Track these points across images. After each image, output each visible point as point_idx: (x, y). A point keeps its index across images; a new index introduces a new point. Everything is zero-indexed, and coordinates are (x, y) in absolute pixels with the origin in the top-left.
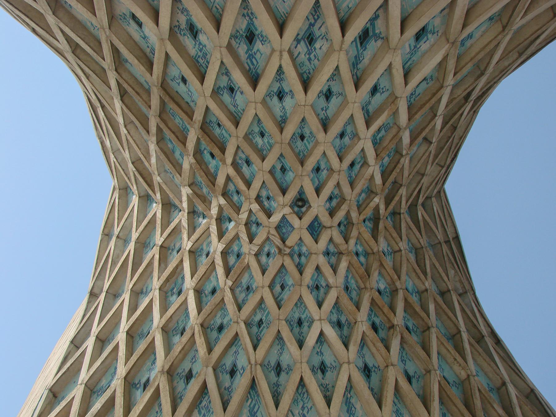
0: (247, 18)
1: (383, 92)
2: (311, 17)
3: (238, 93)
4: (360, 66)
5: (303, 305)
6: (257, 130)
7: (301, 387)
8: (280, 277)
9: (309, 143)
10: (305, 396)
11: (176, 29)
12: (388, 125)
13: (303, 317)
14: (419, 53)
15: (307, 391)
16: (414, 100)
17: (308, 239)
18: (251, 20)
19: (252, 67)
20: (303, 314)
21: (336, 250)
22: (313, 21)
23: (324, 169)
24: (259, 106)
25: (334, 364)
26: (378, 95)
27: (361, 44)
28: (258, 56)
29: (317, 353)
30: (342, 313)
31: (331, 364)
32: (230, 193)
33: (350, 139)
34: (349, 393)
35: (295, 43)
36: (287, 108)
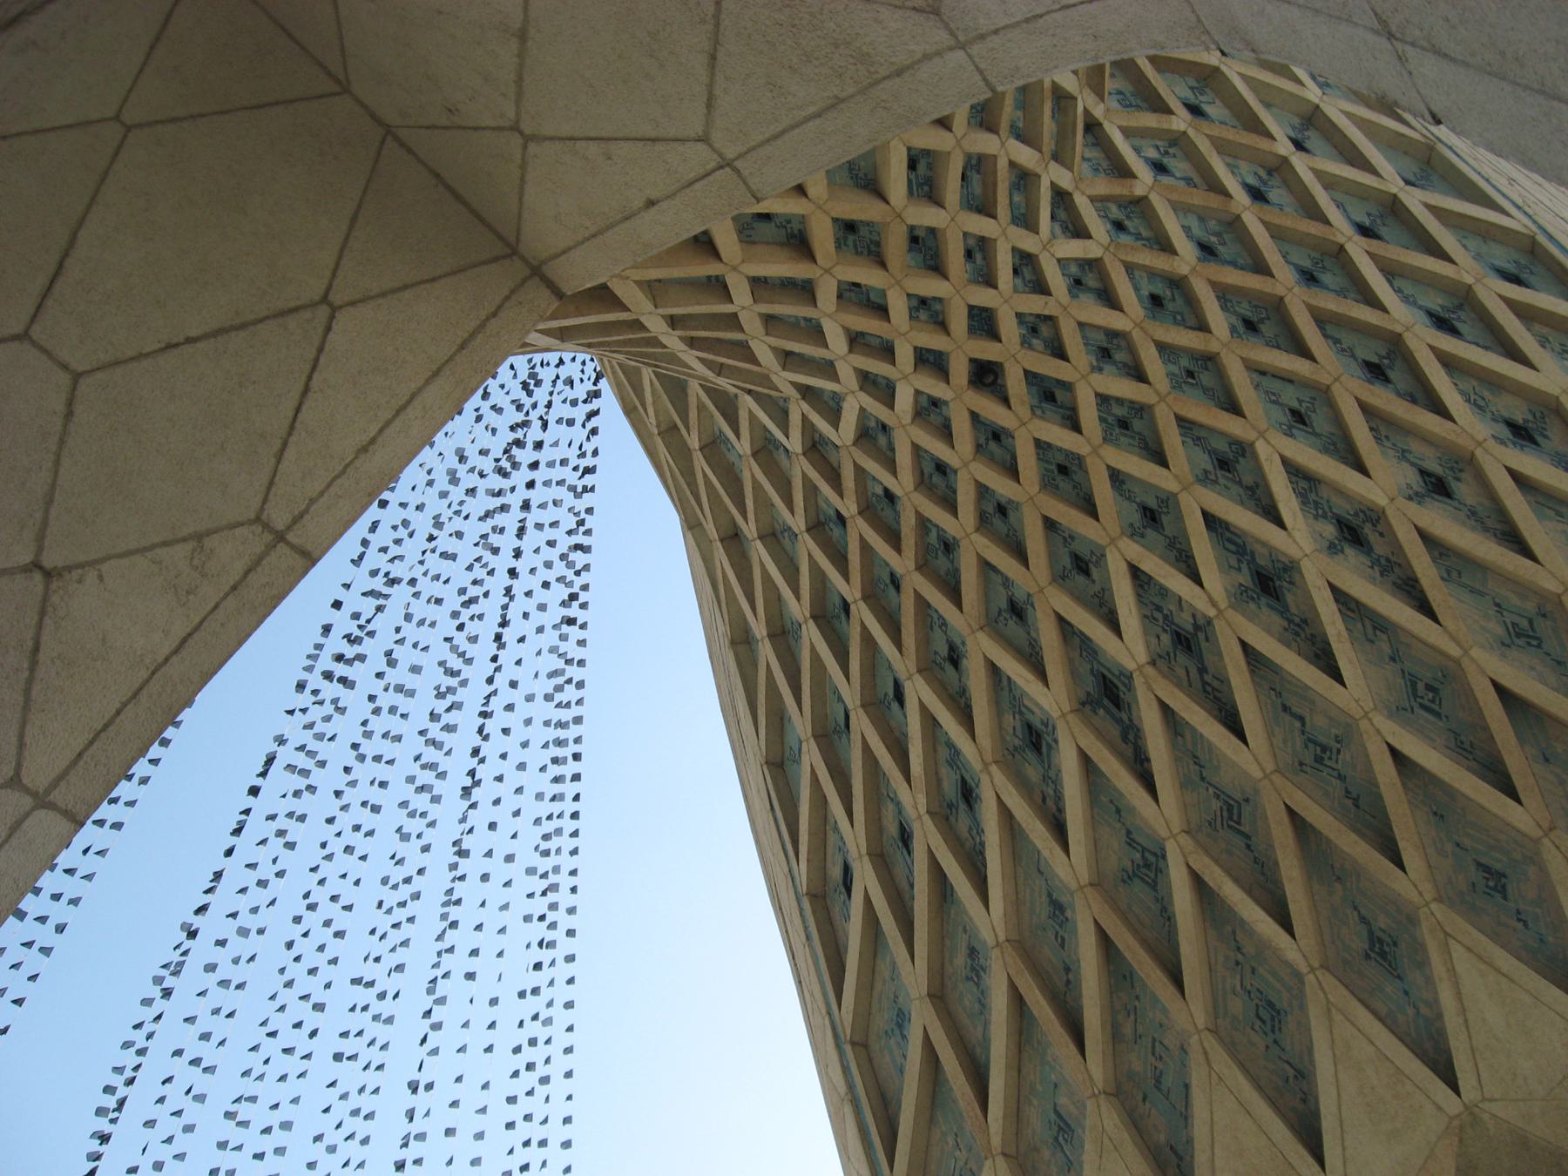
0: (1297, 620)
1: (1000, 614)
2: (1216, 683)
3: (1210, 467)
4: (1077, 641)
6: (1137, 425)
11: (1374, 517)
13: (851, 238)
17: (935, 341)
18: (1290, 621)
19: (1228, 535)
22: (1207, 678)
24: (1172, 486)
26: (1004, 604)
27: (1104, 677)
28: (1233, 561)
35: (1201, 622)
36: (1126, 504)
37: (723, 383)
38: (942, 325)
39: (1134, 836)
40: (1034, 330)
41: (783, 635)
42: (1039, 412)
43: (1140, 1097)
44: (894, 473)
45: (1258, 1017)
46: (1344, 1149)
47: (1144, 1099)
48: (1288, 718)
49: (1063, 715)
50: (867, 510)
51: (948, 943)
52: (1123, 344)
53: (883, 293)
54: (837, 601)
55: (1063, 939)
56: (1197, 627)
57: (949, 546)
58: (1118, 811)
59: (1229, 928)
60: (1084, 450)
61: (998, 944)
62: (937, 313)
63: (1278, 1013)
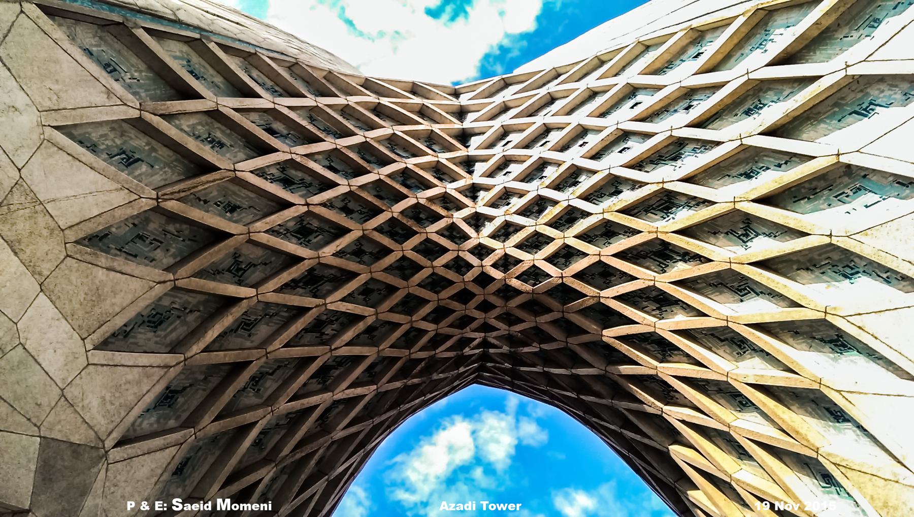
14: (322, 225)
24: (381, 348)
28: (338, 360)
39: (252, 268)
43: (136, 222)
45: (157, 313)
46: (102, 365)
47: (134, 224)
48: (275, 367)
49: (319, 257)
51: (228, 131)
55: (218, 206)
56: (324, 333)
58: (266, 264)
59: (201, 309)
60: (414, 318)
61: (235, 170)
63: (156, 327)
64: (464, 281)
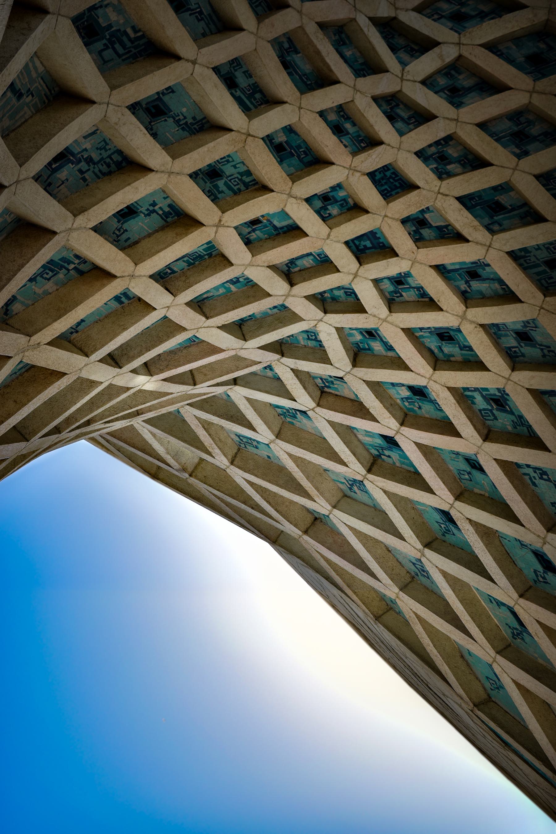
5: (243, 188)
7: (120, 159)
8: (299, 147)
9: (538, 274)
10: (104, 168)
12: (492, 418)
13: (221, 183)
15: (110, 173)
16: (525, 474)
20: (226, 184)
21: (297, 269)
23: (470, 286)
25: (124, 237)
29: (154, 204)
30: (190, 264)
31: (126, 230)
32: (453, 72)
33: (510, 348)
34: (75, 268)
37: (204, 389)
38: (357, 209)
40: (443, 159)
41: (414, 580)
42: (496, 227)
44: (406, 368)
50: (406, 419)
52: (531, 117)
53: (284, 214)
54: (437, 517)
57: (500, 401)
62: (344, 200)
64: (414, 262)
